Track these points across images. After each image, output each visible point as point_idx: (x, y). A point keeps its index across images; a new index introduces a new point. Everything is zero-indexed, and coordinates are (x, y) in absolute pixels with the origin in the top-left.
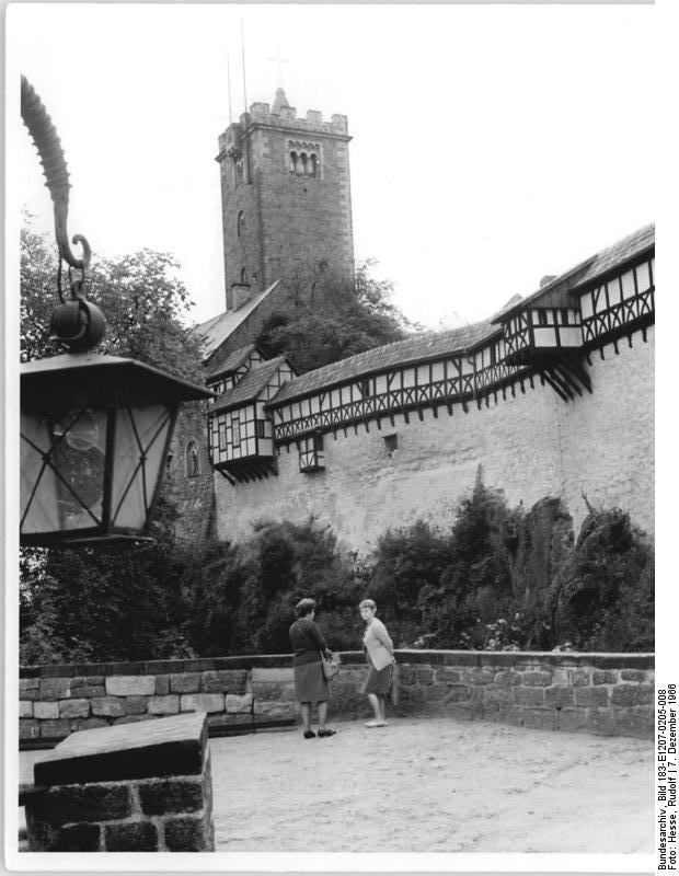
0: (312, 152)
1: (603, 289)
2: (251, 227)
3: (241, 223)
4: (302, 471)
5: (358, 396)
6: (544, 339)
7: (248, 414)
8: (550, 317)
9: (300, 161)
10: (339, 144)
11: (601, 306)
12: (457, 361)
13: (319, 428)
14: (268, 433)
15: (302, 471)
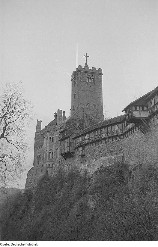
0: (93, 77)
1: (153, 99)
2: (77, 96)
3: (75, 95)
4: (80, 156)
5: (93, 135)
6: (137, 114)
7: (67, 140)
8: (138, 108)
9: (90, 79)
10: (100, 75)
11: (153, 104)
12: (118, 125)
13: (84, 144)
14: (73, 145)
15: (80, 156)
